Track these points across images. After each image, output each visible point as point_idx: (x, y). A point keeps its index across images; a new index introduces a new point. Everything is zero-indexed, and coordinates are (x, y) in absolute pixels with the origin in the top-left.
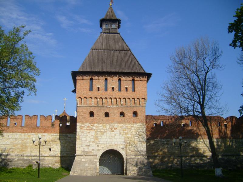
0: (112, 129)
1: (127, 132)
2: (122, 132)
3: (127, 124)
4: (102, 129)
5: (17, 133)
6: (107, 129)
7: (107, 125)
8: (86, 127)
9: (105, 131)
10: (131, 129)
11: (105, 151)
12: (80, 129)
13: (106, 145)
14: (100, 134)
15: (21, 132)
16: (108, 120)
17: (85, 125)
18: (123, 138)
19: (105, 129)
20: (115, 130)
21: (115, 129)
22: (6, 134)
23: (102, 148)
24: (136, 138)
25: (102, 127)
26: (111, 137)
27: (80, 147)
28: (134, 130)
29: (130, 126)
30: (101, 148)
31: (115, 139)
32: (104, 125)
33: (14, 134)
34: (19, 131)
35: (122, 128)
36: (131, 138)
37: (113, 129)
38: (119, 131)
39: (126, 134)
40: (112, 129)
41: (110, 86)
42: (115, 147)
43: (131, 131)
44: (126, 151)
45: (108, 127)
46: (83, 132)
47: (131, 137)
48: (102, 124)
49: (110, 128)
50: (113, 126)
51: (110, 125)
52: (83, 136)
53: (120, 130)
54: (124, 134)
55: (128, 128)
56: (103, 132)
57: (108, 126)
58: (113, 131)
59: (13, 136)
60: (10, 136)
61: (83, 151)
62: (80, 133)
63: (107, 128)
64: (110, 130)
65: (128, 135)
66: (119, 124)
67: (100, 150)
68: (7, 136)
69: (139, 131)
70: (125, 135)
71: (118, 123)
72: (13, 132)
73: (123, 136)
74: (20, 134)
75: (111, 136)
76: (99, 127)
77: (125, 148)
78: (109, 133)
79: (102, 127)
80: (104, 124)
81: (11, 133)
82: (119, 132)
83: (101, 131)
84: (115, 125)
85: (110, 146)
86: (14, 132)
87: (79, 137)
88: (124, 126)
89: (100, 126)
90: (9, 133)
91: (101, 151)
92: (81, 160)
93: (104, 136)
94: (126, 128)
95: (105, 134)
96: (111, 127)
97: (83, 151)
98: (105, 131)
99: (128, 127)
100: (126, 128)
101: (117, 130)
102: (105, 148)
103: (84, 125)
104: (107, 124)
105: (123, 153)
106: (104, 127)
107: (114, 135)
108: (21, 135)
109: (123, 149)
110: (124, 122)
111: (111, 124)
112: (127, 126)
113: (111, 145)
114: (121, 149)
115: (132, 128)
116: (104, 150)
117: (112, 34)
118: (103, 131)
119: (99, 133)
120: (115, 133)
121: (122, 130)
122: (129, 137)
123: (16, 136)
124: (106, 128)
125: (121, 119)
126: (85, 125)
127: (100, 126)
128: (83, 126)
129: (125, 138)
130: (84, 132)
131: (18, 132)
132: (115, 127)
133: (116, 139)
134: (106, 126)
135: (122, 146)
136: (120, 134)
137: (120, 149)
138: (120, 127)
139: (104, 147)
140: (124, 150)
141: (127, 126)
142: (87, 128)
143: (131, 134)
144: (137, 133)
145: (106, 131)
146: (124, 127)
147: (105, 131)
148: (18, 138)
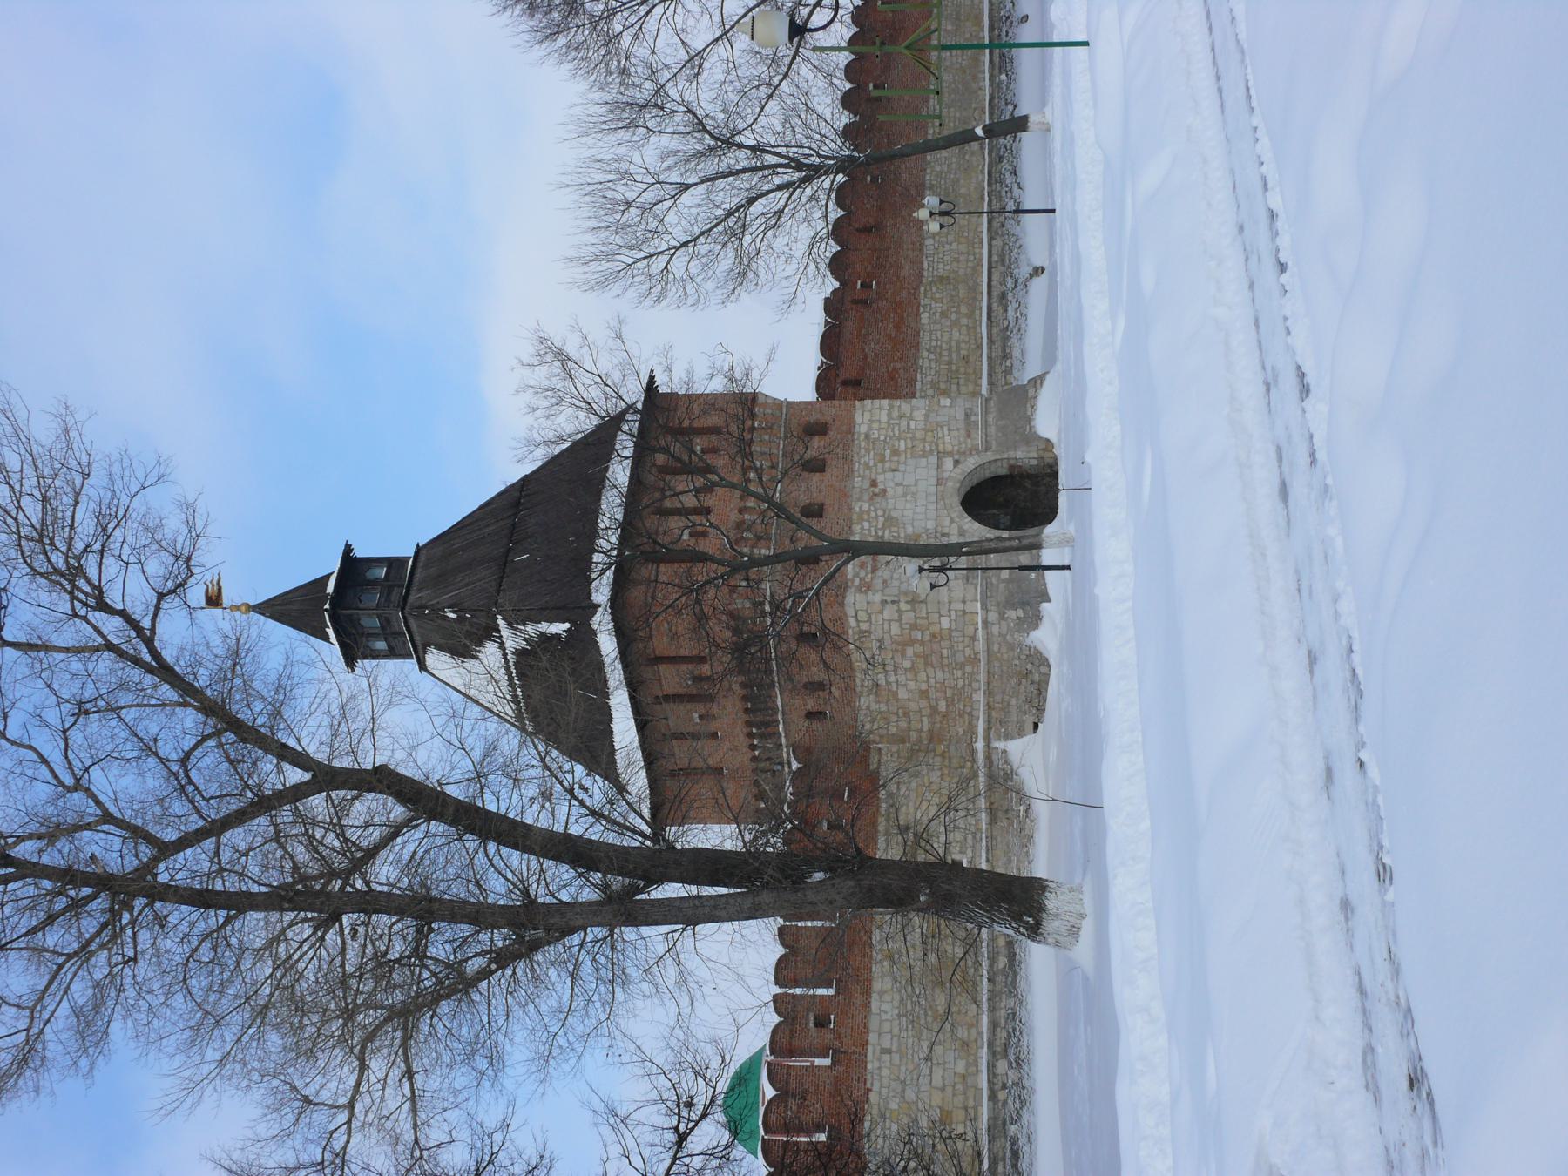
0: (876, 495)
1: (888, 452)
2: (887, 465)
3: (855, 449)
4: (874, 524)
5: (869, 1012)
6: (876, 510)
7: (857, 509)
8: (862, 574)
9: (884, 516)
10: (875, 440)
11: (966, 515)
12: (870, 593)
13: (941, 512)
14: (896, 529)
15: (867, 992)
16: (836, 507)
17: (856, 575)
18: (911, 462)
19: (873, 514)
20: (881, 486)
21: (874, 484)
22: (876, 1064)
23: (952, 521)
24: (912, 426)
25: (866, 525)
26: (909, 497)
27: (950, 590)
28: (883, 432)
29: (863, 444)
30: (954, 525)
31: (916, 485)
32: (855, 517)
33: (874, 1023)
34: (858, 1001)
35: (871, 464)
36: (913, 439)
37: (876, 490)
38: (884, 472)
39: (895, 452)
40: (876, 495)
41: (689, 501)
42: (950, 484)
43: (885, 441)
44: (964, 453)
45: (866, 506)
46: (885, 582)
47: (909, 441)
48: (851, 524)
49: (871, 499)
50: (861, 492)
51: (859, 499)
52: (901, 583)
53: (880, 471)
54: (896, 459)
55: (874, 449)
56: (886, 520)
57: (860, 508)
58: (884, 491)
59: (886, 1027)
60: (886, 1045)
61: (968, 580)
62: (887, 591)
63: (870, 510)
64: (878, 499)
65: (902, 447)
66: (856, 474)
67: (960, 528)
68: (886, 1057)
69: (884, 418)
70: (902, 458)
71: (849, 475)
72: (866, 1030)
73: (905, 463)
74: (874, 996)
75: (905, 495)
76: (866, 532)
77: (956, 457)
78: (891, 501)
79: (866, 525)
80: (851, 519)
81: (872, 1038)
82: (889, 475)
83: (880, 526)
84: (856, 485)
85: (943, 499)
86: (866, 1026)
87: (906, 594)
88: (863, 458)
89: (862, 529)
90: (870, 1048)
91: (966, 527)
92: (1003, 581)
93: (903, 516)
94: (872, 453)
95: (894, 514)
96: (866, 497)
97: (968, 580)
98: (884, 516)
99: (867, 450)
100: (872, 453)
101: (880, 478)
102: (954, 515)
103: (853, 581)
104: (850, 508)
105: (971, 463)
106: (865, 517)
107: (900, 490)
108: (881, 993)
109: (957, 463)
110: (847, 460)
111: (855, 496)
112: (863, 451)
113: (940, 497)
114: (960, 466)
115: (876, 436)
116: (961, 517)
117: (419, 570)
118: (881, 520)
119: (890, 532)
120: (892, 484)
121: (880, 465)
122: (910, 446)
123: (884, 1017)
124: (868, 512)
125: (835, 470)
126: (854, 576)
127: (862, 529)
128: (857, 582)
129: (912, 457)
130: (885, 577)
131: (866, 1005)
132: (867, 485)
133: (916, 481)
134: (862, 512)
135: (948, 463)
136: (895, 470)
137: (958, 470)
138: (868, 472)
139: (948, 519)
140: (962, 459)
141: (863, 451)
142: (869, 569)
143: (899, 439)
144: (892, 422)
145: (884, 511)
146: (869, 459)
147: (880, 513)
148: (896, 1003)
